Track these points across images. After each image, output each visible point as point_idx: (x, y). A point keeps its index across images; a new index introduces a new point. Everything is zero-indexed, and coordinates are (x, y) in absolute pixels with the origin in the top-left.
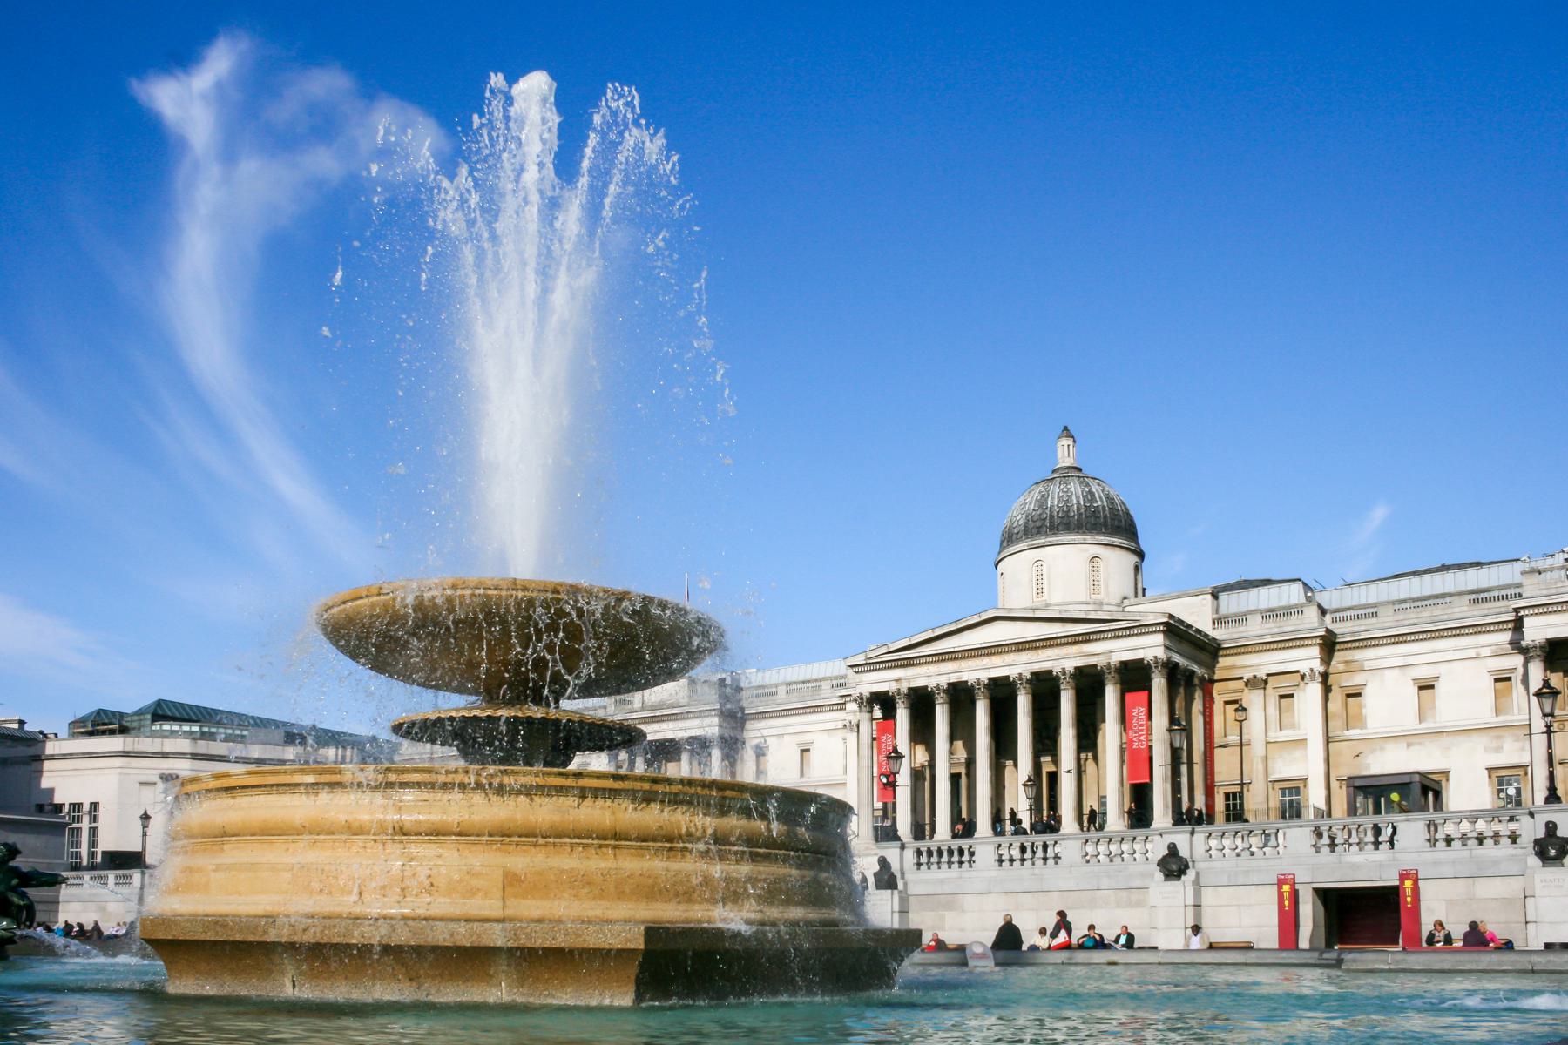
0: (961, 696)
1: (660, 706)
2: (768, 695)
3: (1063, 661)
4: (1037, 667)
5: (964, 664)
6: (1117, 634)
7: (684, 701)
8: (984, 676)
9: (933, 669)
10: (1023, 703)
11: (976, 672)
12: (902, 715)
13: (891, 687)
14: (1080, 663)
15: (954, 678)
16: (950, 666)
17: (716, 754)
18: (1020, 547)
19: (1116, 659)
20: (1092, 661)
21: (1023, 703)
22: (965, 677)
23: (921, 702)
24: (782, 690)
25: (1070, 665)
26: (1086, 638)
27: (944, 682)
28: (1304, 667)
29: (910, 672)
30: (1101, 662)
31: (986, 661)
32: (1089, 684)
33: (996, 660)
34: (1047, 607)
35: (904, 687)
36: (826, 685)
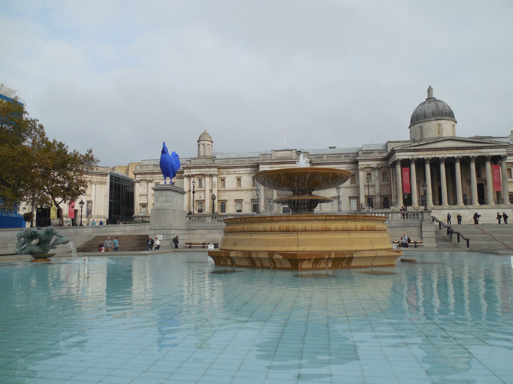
0: (435, 163)
1: (283, 158)
2: (320, 157)
3: (473, 154)
4: (463, 155)
5: (438, 152)
6: (491, 147)
7: (294, 158)
8: (445, 156)
9: (425, 153)
10: (458, 165)
12: (413, 167)
13: (411, 158)
14: (478, 155)
15: (433, 156)
16: (434, 152)
18: (432, 119)
19: (490, 154)
21: (458, 165)
22: (437, 156)
23: (420, 163)
24: (325, 158)
25: (475, 155)
26: (481, 148)
27: (430, 157)
29: (417, 153)
30: (486, 155)
31: (445, 152)
32: (481, 161)
33: (450, 152)
34: (455, 137)
35: (415, 157)
36: (342, 156)
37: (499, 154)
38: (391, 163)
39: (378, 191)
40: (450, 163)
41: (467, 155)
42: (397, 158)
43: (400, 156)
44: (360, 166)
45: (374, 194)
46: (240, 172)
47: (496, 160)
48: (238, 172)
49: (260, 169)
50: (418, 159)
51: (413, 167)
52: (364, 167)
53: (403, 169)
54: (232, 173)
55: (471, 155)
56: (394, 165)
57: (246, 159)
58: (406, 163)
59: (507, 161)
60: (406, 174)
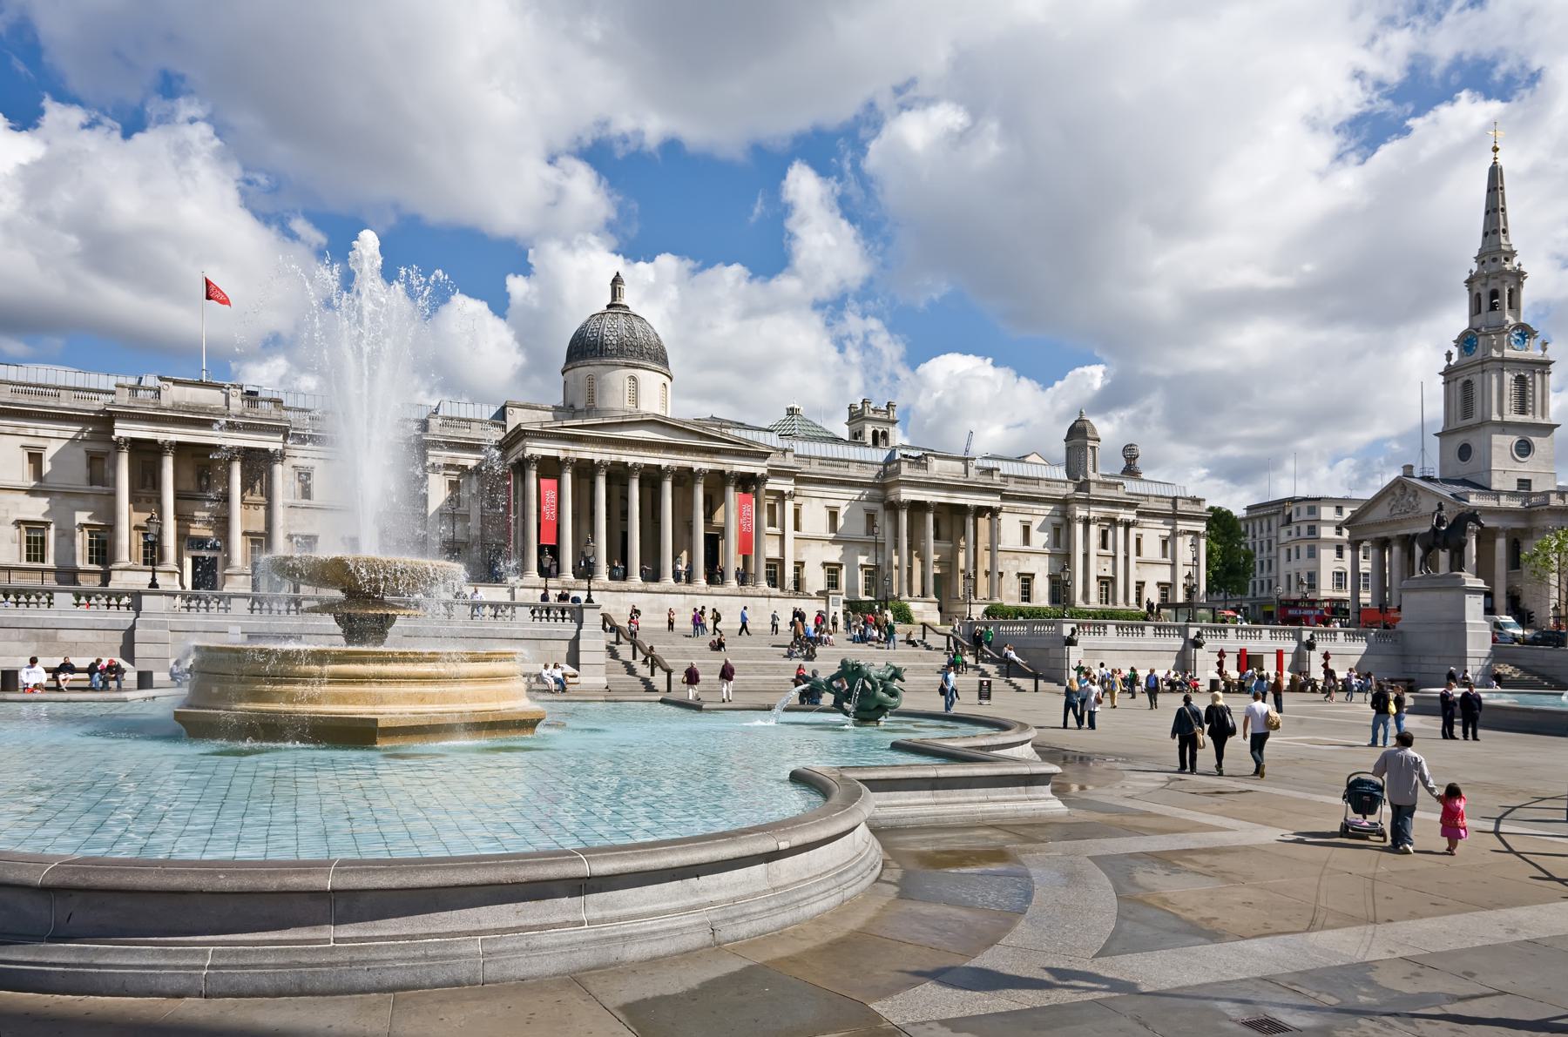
0: (618, 475)
4: (680, 463)
10: (668, 486)
11: (631, 457)
12: (567, 478)
13: (562, 455)
15: (614, 458)
17: (278, 469)
19: (736, 469)
20: (720, 467)
21: (668, 486)
22: (624, 459)
23: (585, 472)
26: (717, 452)
27: (606, 458)
28: (786, 489)
30: (728, 469)
32: (718, 483)
35: (571, 455)
37: (752, 470)
38: (512, 460)
39: (475, 532)
40: (652, 478)
41: (688, 464)
42: (529, 452)
43: (536, 449)
44: (431, 460)
45: (464, 538)
46: (41, 433)
47: (747, 482)
48: (32, 432)
49: (118, 433)
50: (579, 460)
51: (567, 478)
52: (441, 462)
53: (542, 481)
54: (8, 430)
55: (696, 467)
56: (521, 467)
57: (63, 393)
58: (550, 468)
59: (768, 487)
60: (550, 495)
